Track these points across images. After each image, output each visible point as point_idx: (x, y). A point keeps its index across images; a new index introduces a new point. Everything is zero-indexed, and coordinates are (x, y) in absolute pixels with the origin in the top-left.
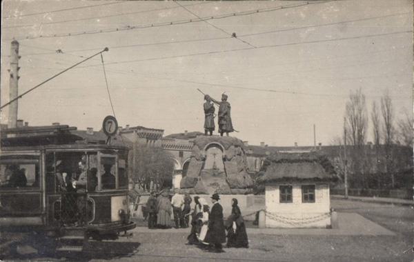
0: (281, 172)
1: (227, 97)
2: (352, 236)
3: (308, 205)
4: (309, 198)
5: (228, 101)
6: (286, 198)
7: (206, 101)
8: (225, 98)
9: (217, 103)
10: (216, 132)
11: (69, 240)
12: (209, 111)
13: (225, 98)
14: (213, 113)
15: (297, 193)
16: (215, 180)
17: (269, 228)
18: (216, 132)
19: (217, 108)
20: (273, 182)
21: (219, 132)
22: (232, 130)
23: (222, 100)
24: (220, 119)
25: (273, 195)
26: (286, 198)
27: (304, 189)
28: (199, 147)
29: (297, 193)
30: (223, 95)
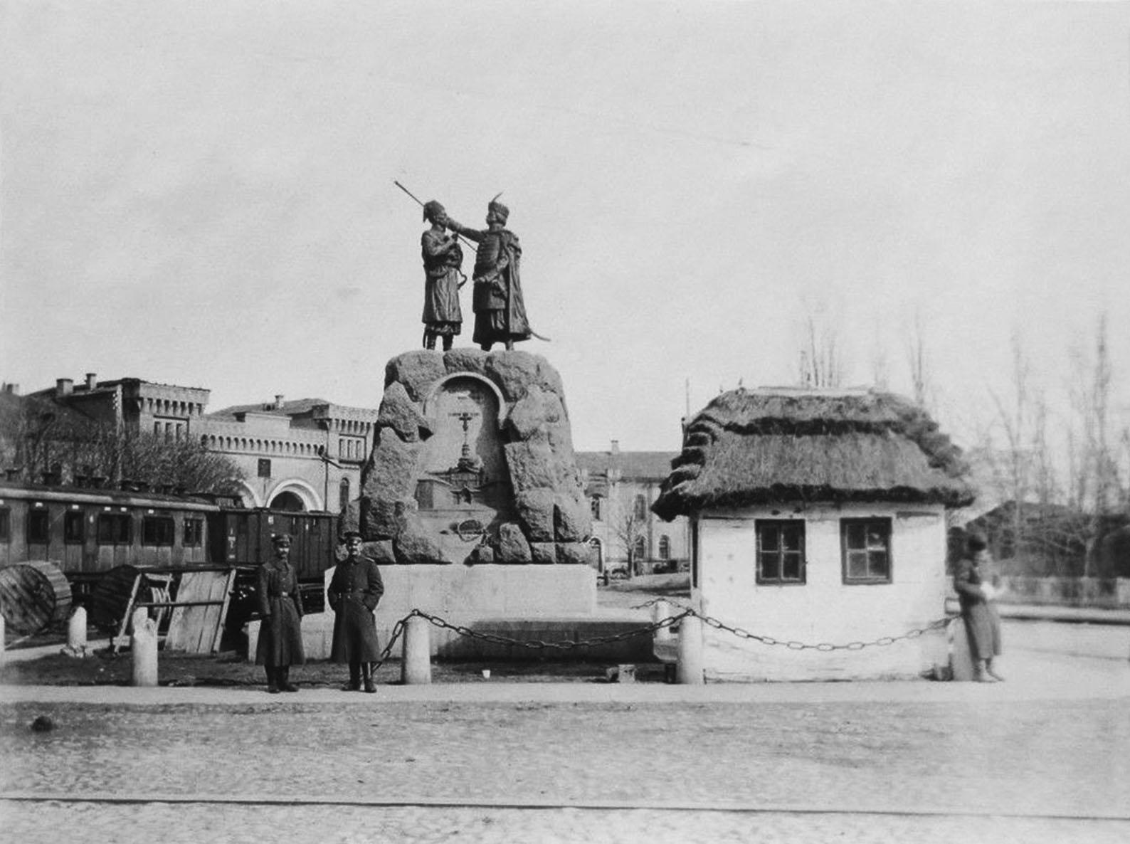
0: (760, 464)
1: (506, 212)
2: (929, 775)
3: (869, 595)
4: (869, 555)
5: (509, 226)
6: (781, 561)
7: (428, 225)
8: (497, 213)
9: (471, 234)
10: (465, 341)
11: (431, 301)
12: (438, 262)
13: (497, 213)
14: (458, 267)
15: (823, 540)
16: (469, 512)
17: (719, 681)
18: (465, 341)
19: (469, 251)
20: (728, 504)
21: (476, 339)
22: (524, 335)
23: (490, 222)
24: (482, 292)
25: (729, 548)
26: (781, 561)
27: (854, 533)
28: (409, 390)
29: (823, 540)
30: (493, 206)
